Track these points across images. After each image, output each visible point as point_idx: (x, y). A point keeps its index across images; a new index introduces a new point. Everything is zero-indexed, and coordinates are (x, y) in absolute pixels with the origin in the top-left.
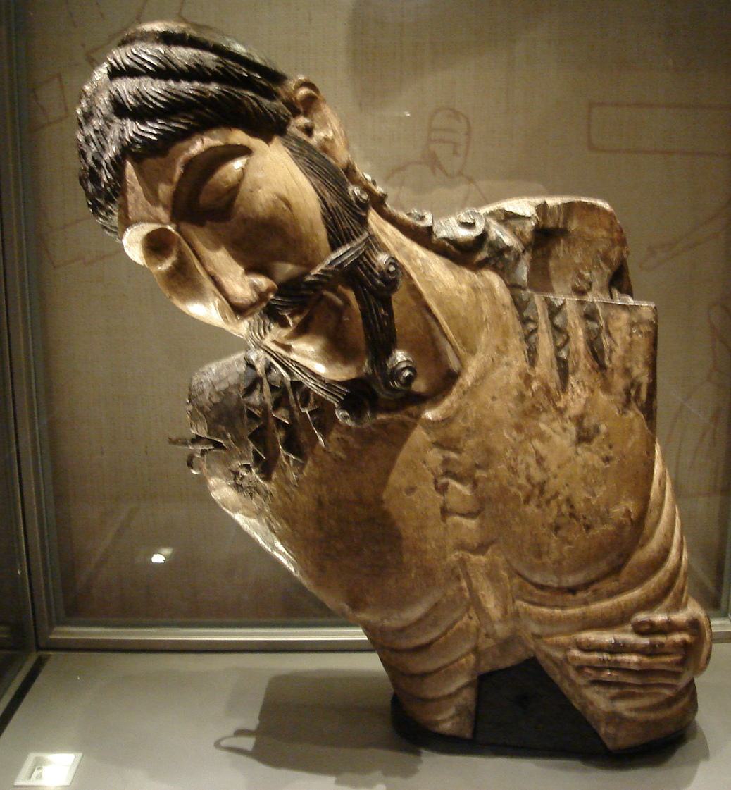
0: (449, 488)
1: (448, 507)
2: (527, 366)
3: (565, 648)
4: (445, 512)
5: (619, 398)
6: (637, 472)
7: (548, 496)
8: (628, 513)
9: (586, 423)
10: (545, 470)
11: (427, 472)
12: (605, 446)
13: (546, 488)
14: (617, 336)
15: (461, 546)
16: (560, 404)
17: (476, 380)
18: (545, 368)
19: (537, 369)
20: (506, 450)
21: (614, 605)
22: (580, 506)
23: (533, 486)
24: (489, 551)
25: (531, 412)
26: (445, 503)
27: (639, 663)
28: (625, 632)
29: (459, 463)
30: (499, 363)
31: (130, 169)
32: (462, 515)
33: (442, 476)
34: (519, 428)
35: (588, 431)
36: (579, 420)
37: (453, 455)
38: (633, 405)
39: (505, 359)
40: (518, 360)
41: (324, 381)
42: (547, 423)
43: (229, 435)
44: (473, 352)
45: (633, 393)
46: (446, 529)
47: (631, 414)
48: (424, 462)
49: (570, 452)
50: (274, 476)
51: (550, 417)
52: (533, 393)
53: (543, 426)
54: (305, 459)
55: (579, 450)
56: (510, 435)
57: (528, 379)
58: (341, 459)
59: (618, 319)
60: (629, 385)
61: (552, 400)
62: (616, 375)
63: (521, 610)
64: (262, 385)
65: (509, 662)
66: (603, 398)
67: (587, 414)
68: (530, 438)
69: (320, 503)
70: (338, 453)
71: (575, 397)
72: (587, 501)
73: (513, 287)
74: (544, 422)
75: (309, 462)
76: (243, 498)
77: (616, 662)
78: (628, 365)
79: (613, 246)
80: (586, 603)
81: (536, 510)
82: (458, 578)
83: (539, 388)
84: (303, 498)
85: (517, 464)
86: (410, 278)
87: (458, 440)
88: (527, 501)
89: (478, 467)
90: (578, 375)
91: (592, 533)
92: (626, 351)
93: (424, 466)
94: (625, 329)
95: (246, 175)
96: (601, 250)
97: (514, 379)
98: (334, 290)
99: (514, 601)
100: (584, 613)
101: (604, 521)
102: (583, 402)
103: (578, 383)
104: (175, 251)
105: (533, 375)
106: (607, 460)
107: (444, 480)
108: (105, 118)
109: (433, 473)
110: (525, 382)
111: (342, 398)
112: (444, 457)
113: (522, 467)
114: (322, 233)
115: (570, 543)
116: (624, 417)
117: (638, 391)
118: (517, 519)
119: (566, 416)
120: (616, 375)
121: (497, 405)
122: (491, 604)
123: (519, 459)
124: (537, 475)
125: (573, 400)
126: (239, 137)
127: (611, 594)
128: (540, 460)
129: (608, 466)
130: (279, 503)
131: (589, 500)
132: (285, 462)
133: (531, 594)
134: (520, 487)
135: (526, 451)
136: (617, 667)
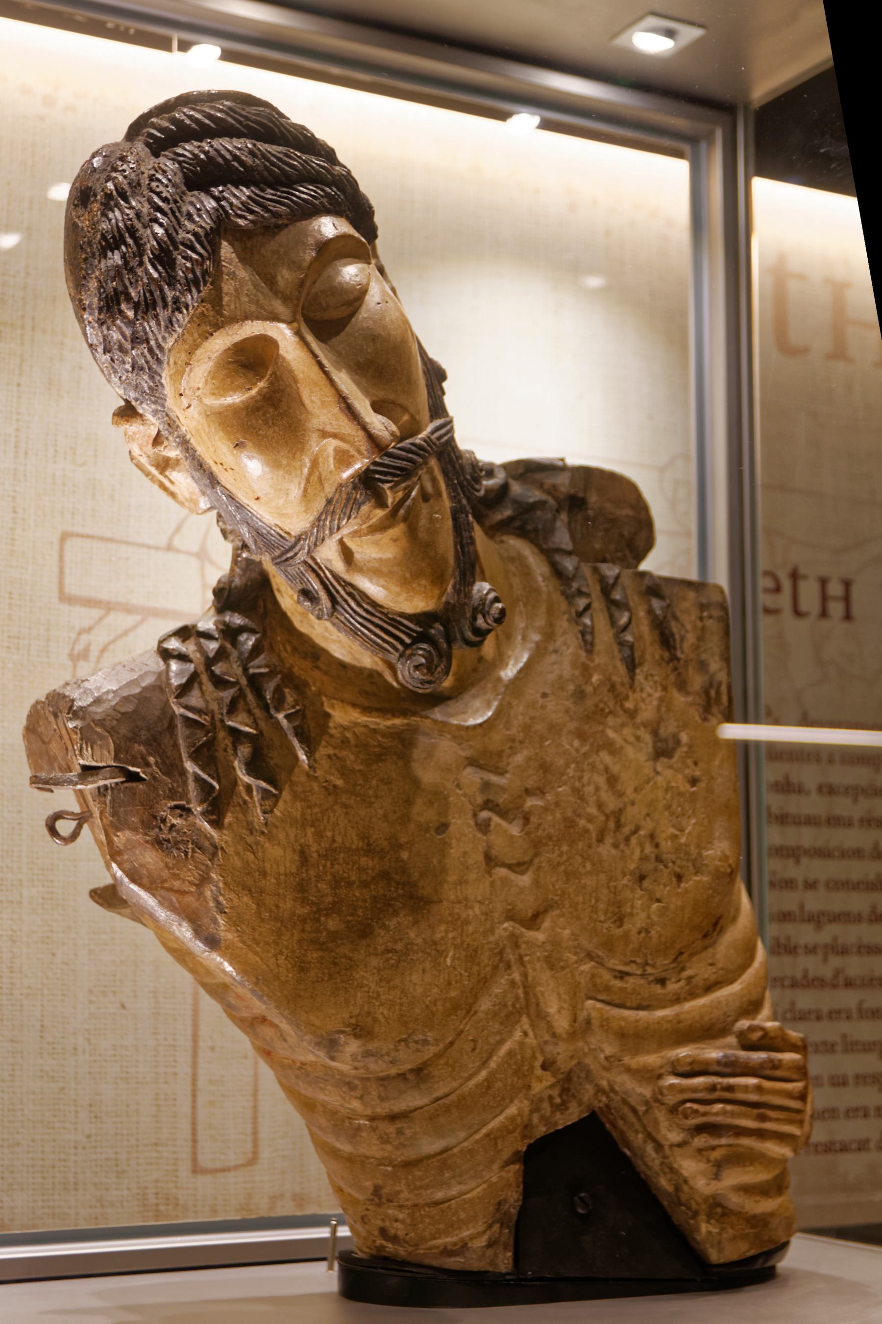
0: (493, 824)
1: (494, 852)
2: (583, 654)
3: (652, 1076)
4: (491, 861)
7: (626, 830)
9: (662, 731)
10: (621, 795)
11: (463, 799)
12: (689, 762)
13: (623, 820)
15: (510, 916)
16: (629, 705)
18: (607, 658)
19: (597, 660)
20: (567, 766)
21: (712, 1001)
22: (666, 845)
23: (607, 817)
24: (546, 924)
25: (595, 713)
27: (759, 1089)
29: (503, 789)
30: (546, 649)
31: (226, 250)
32: (510, 867)
33: (482, 809)
34: (581, 736)
35: (665, 740)
37: (494, 778)
38: (715, 709)
40: (568, 644)
41: (386, 615)
42: (618, 729)
43: (151, 760)
46: (492, 884)
48: (458, 786)
49: (648, 770)
50: (228, 819)
51: (619, 721)
52: (594, 689)
53: (611, 734)
55: (659, 769)
56: (572, 746)
57: (586, 671)
58: (335, 786)
59: (684, 599)
61: (620, 699)
63: (594, 1014)
64: (201, 684)
66: (679, 699)
69: (304, 857)
71: (644, 695)
72: (674, 837)
73: (549, 554)
74: (611, 727)
75: (286, 795)
76: (171, 862)
77: (730, 1088)
80: (678, 1000)
81: (614, 851)
82: (509, 967)
83: (602, 683)
85: (583, 786)
87: (500, 754)
88: (600, 840)
89: (528, 792)
90: (645, 668)
92: (699, 639)
93: (458, 791)
96: (626, 533)
97: (567, 669)
99: (583, 1002)
100: (677, 1015)
102: (655, 703)
103: (646, 678)
105: (592, 665)
106: (694, 781)
107: (485, 814)
109: (470, 803)
111: (408, 641)
112: (482, 779)
113: (589, 789)
115: (658, 901)
116: (706, 723)
117: (718, 693)
118: (588, 866)
119: (638, 720)
120: (691, 671)
121: (551, 705)
122: (554, 1007)
123: (585, 780)
124: (612, 804)
125: (643, 700)
128: (612, 780)
129: (694, 789)
131: (676, 836)
132: (247, 798)
133: (607, 989)
134: (590, 820)
135: (593, 767)
136: (728, 1095)
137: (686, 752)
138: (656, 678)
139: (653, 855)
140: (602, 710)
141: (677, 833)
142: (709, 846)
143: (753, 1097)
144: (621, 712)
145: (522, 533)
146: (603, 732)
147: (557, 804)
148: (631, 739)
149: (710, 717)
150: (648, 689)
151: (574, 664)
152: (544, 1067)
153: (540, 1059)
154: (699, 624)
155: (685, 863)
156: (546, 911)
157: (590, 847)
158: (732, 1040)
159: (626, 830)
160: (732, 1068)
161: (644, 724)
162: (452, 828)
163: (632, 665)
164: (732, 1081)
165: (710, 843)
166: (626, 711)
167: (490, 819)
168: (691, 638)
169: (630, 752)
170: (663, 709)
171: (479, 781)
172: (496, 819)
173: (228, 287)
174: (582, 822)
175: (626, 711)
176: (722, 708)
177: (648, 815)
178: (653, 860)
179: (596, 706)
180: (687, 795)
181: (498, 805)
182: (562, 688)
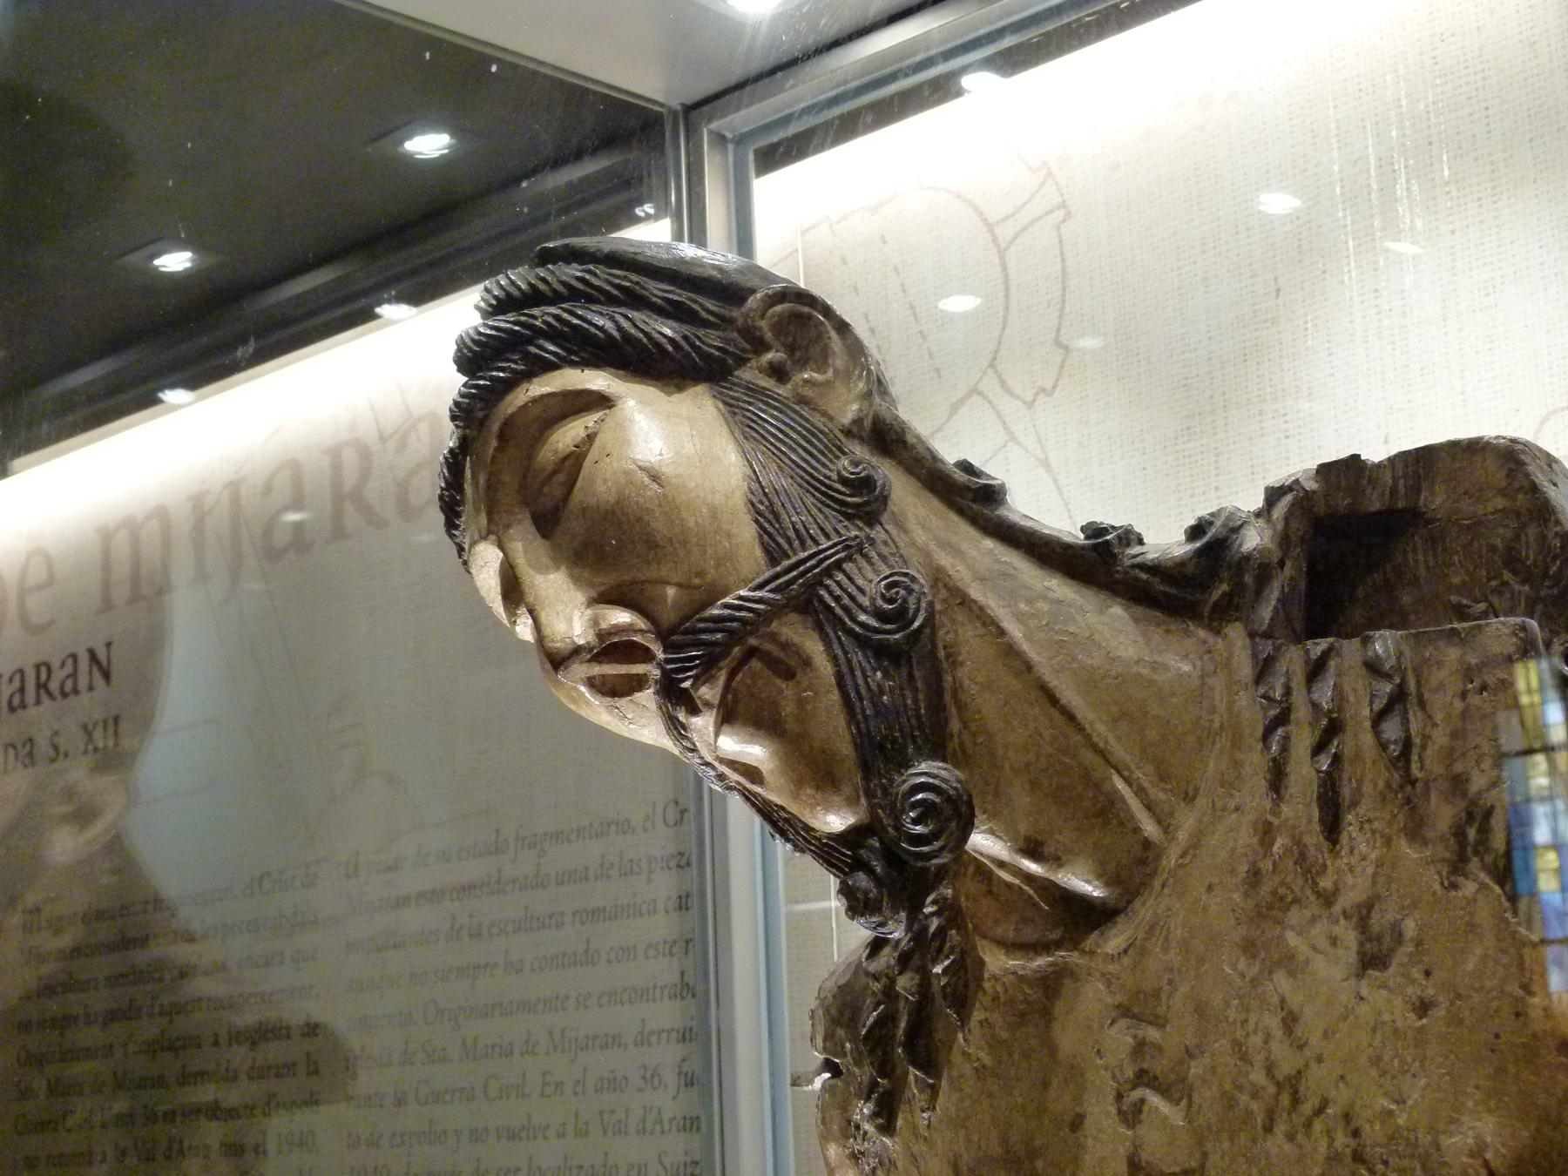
0: (1146, 1109)
1: (1144, 1156)
5: (1440, 847)
6: (1497, 1036)
7: (1307, 1108)
8: (1478, 1152)
9: (1375, 918)
12: (1416, 973)
14: (1437, 702)
16: (1326, 883)
18: (1300, 808)
20: (1227, 1005)
22: (1373, 1132)
23: (1278, 1084)
25: (1270, 907)
26: (1136, 1147)
34: (1249, 948)
35: (1379, 938)
36: (1362, 916)
37: (1152, 1033)
38: (1474, 864)
40: (1254, 794)
41: (819, 839)
44: (1189, 798)
45: (1472, 833)
47: (1469, 888)
50: (900, 1122)
51: (1307, 913)
52: (1274, 864)
53: (1292, 939)
54: (938, 1077)
55: (1364, 992)
56: (1234, 967)
57: (1266, 833)
59: (1440, 664)
60: (1463, 815)
61: (1311, 873)
62: (1433, 796)
67: (1379, 897)
70: (982, 1055)
74: (1292, 928)
75: (944, 1083)
78: (1458, 767)
79: (1523, 527)
81: (1287, 1147)
83: (1287, 851)
85: (1247, 1035)
86: (1002, 632)
88: (1268, 1129)
90: (1361, 810)
92: (1454, 735)
93: (1099, 1062)
94: (1454, 686)
97: (1246, 838)
102: (1370, 870)
105: (1276, 822)
106: (1423, 1008)
107: (1138, 1093)
109: (1114, 1077)
110: (1262, 842)
112: (1135, 1037)
117: (1484, 830)
119: (1337, 908)
123: (1251, 1026)
126: (597, 380)
128: (1290, 1021)
129: (1424, 1021)
131: (1390, 1113)
137: (1411, 954)
138: (1376, 825)
139: (1348, 1151)
140: (1282, 899)
141: (1393, 1107)
142: (1452, 1127)
144: (1313, 898)
146: (1281, 937)
148: (1323, 943)
149: (1461, 880)
150: (1363, 847)
154: (1459, 705)
155: (1406, 1162)
157: (1254, 1141)
159: (1307, 1108)
162: (1088, 1122)
165: (1453, 1121)
167: (1142, 1101)
168: (1440, 738)
170: (1381, 879)
171: (1130, 1040)
172: (1154, 1100)
174: (1244, 1098)
175: (1318, 894)
176: (1488, 859)
178: (1348, 1160)
179: (1274, 893)
180: (1410, 1033)
181: (1156, 1078)
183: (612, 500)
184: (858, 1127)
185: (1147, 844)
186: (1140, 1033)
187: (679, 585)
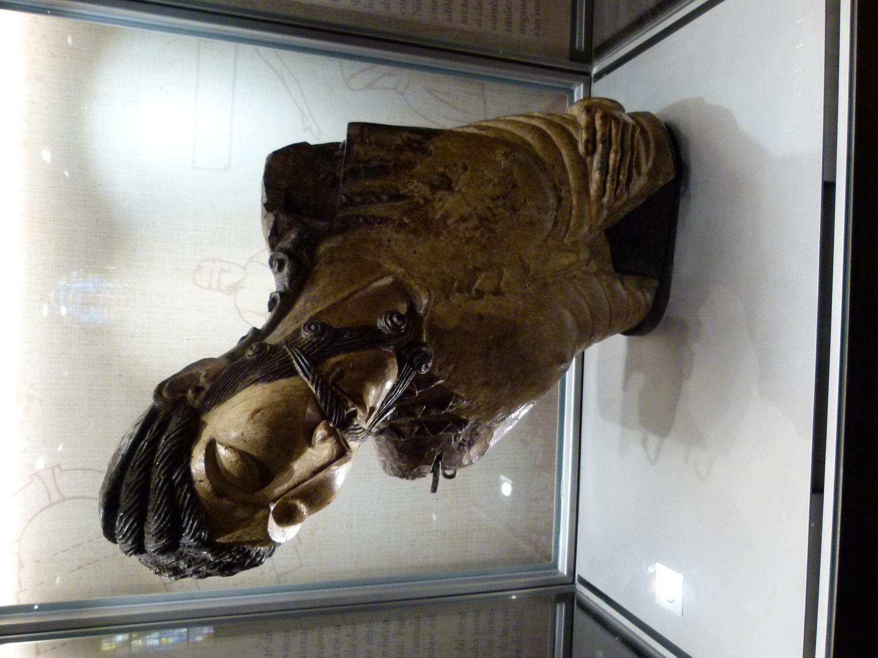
1: (493, 289)
4: (497, 292)
7: (489, 215)
8: (506, 155)
9: (437, 183)
10: (470, 216)
16: (422, 202)
17: (401, 265)
20: (454, 245)
22: (498, 191)
24: (527, 261)
26: (490, 292)
27: (616, 153)
28: (592, 162)
32: (500, 280)
34: (438, 235)
36: (434, 188)
37: (455, 285)
39: (386, 242)
45: (415, 145)
47: (432, 147)
48: (460, 306)
49: (458, 196)
50: (464, 417)
53: (437, 216)
54: (453, 394)
55: (457, 189)
57: (401, 226)
59: (358, 153)
65: (607, 250)
66: (419, 168)
68: (446, 226)
69: (486, 384)
72: (494, 186)
73: (330, 234)
75: (455, 391)
78: (394, 147)
80: (569, 191)
81: (500, 224)
84: (481, 397)
85: (465, 237)
86: (321, 312)
87: (444, 281)
88: (493, 231)
89: (465, 267)
91: (519, 184)
95: (232, 445)
97: (401, 237)
98: (329, 374)
101: (511, 174)
102: (420, 184)
103: (406, 187)
104: (292, 502)
106: (465, 168)
107: (473, 292)
108: (178, 559)
113: (467, 234)
114: (283, 382)
117: (415, 141)
118: (505, 240)
119: (430, 198)
120: (402, 158)
121: (420, 249)
122: (565, 260)
123: (461, 235)
124: (475, 222)
125: (419, 192)
127: (564, 171)
128: (463, 219)
130: (483, 414)
134: (482, 235)
136: (618, 170)
143: (619, 154)
145: (316, 246)
147: (473, 253)
148: (441, 204)
150: (412, 187)
151: (398, 232)
152: (587, 265)
153: (584, 268)
154: (374, 146)
156: (522, 261)
158: (588, 159)
159: (489, 215)
160: (604, 168)
161: (433, 194)
163: (397, 197)
164: (611, 167)
166: (425, 204)
167: (476, 290)
168: (382, 154)
169: (448, 206)
171: (457, 294)
172: (476, 285)
173: (246, 538)
174: (484, 241)
177: (482, 200)
182: (411, 241)
183: (266, 429)
184: (460, 444)
185: (392, 284)
186: (455, 290)
187: (306, 405)
